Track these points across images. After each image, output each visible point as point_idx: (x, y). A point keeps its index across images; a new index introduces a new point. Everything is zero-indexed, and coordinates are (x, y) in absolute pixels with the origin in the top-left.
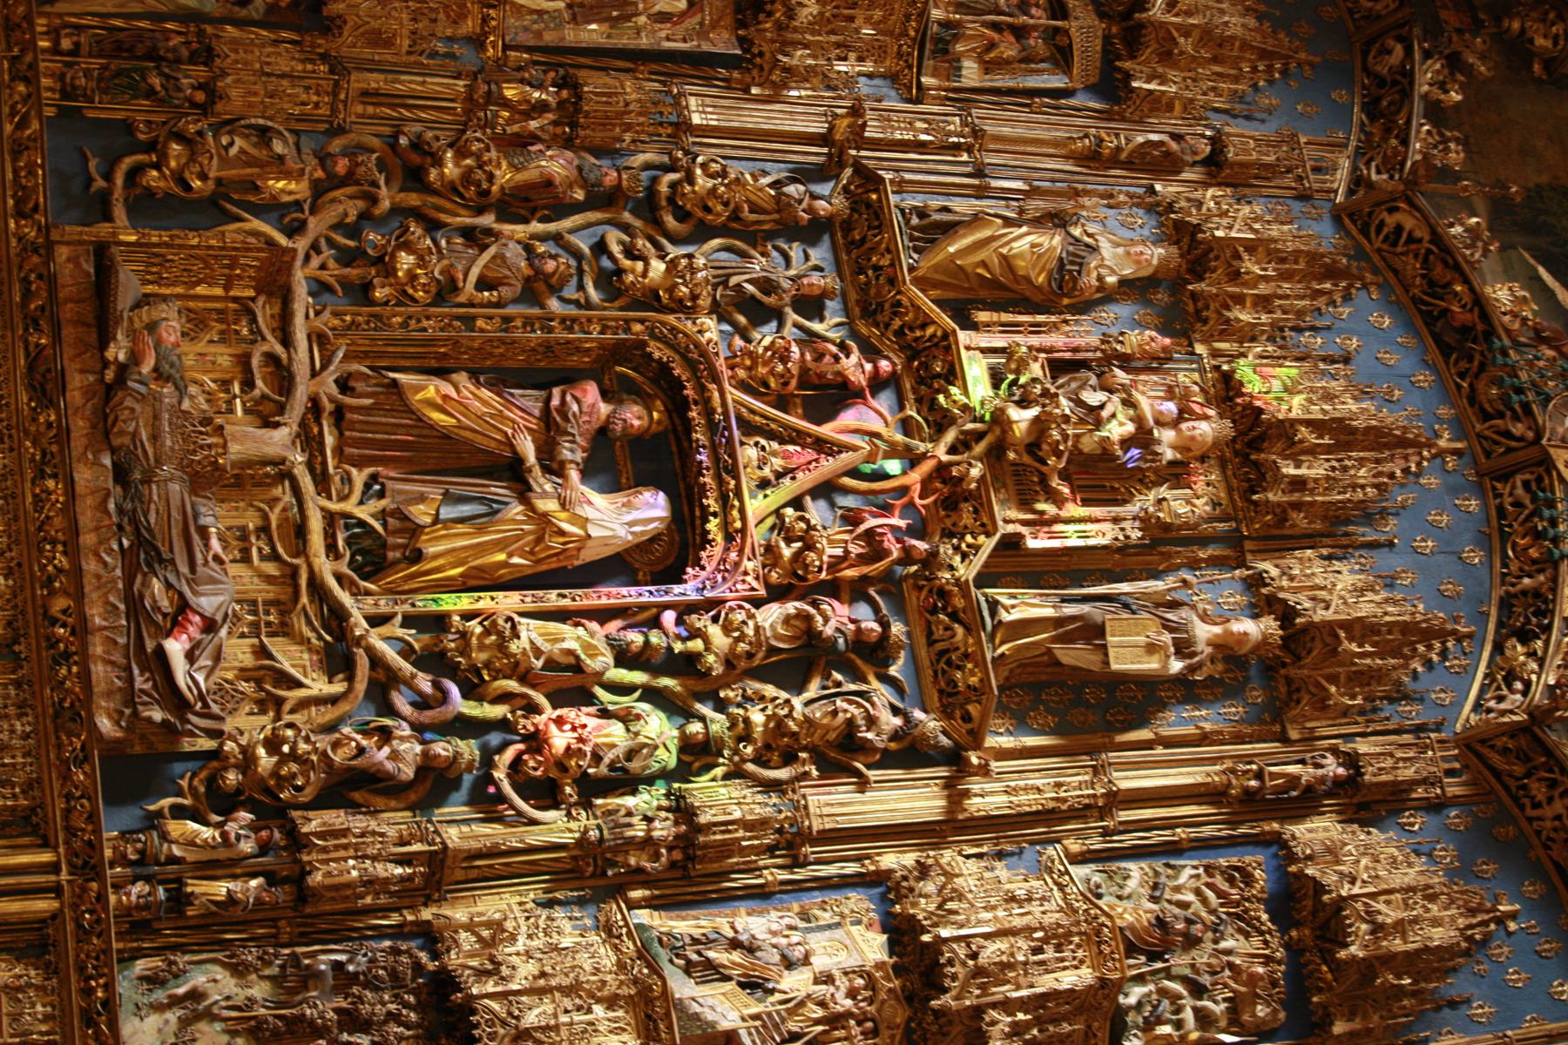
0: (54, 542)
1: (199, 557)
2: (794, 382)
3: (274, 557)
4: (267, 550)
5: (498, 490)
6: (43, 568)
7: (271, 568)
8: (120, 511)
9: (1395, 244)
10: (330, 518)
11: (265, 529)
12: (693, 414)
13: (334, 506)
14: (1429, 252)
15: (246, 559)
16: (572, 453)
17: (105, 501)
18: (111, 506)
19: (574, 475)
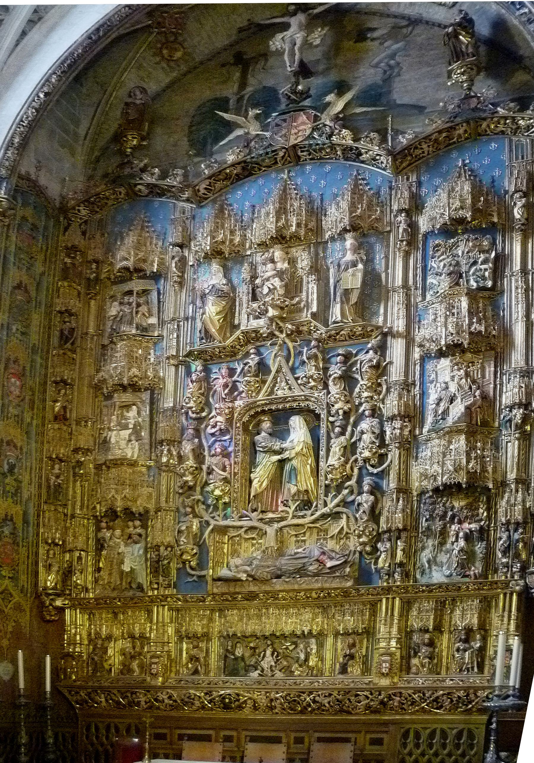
0: (297, 596)
1: (303, 555)
2: (257, 379)
3: (304, 533)
4: (302, 535)
5: (287, 467)
6: (304, 599)
7: (308, 534)
8: (288, 577)
9: (211, 190)
10: (294, 517)
11: (296, 536)
12: (266, 409)
13: (291, 516)
14: (214, 180)
15: (304, 541)
16: (277, 445)
17: (286, 582)
18: (287, 580)
19: (283, 446)
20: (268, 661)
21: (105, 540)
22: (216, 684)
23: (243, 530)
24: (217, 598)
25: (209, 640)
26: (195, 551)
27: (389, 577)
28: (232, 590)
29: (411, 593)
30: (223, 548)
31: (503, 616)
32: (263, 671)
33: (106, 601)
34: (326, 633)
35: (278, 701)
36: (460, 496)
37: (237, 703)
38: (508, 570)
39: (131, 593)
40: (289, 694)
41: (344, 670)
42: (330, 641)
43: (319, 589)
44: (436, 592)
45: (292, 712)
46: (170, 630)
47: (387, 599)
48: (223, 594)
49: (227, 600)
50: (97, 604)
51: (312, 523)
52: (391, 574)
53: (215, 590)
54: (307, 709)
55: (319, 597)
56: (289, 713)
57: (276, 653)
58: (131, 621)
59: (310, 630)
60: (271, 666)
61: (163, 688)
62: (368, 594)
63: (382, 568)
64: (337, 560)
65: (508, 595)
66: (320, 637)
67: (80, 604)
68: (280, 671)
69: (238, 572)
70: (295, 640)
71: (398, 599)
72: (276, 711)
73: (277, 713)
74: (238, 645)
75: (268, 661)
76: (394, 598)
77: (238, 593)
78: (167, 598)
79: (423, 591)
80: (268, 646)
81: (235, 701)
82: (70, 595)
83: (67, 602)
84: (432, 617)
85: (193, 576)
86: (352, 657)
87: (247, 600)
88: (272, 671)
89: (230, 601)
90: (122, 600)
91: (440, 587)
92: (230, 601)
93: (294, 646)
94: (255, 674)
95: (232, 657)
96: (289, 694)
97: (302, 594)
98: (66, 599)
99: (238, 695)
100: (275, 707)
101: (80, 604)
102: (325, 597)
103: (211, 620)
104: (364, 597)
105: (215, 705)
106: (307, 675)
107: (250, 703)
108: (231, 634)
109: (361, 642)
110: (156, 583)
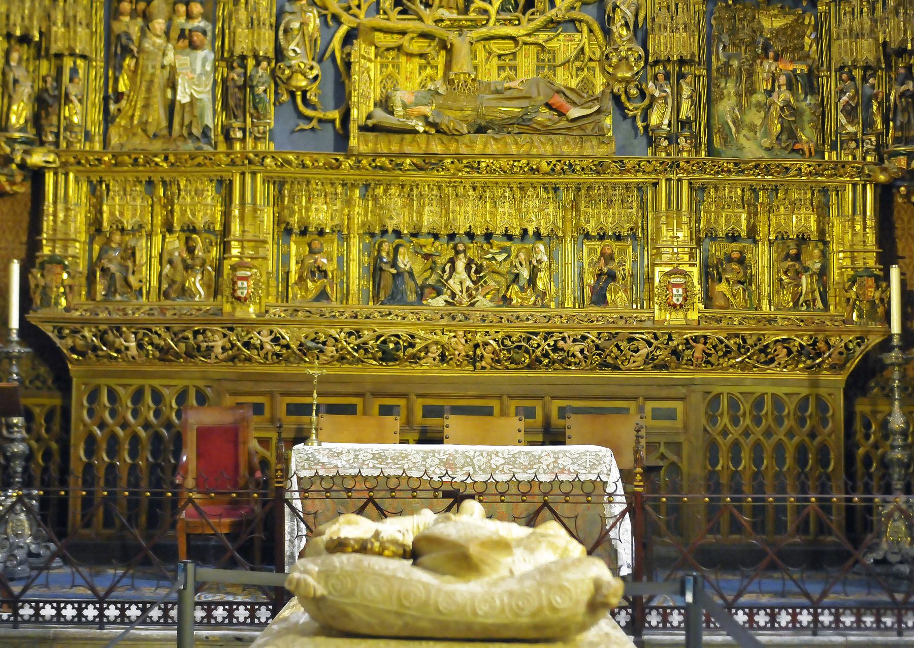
20: (460, 280)
21: (129, 38)
22: (367, 318)
23: (407, 37)
24: (364, 162)
25: (344, 237)
26: (315, 72)
27: (669, 144)
28: (395, 148)
29: (709, 173)
30: (368, 70)
31: (853, 221)
32: (453, 295)
33: (136, 160)
34: (561, 234)
35: (489, 347)
36: (772, 12)
37: (410, 351)
38: (858, 147)
39: (190, 146)
40: (510, 337)
41: (600, 298)
42: (569, 246)
43: (554, 155)
44: (748, 175)
45: (513, 366)
46: (267, 217)
47: (668, 180)
48: (376, 155)
49: (381, 168)
50: (116, 165)
51: (529, 35)
52: (672, 139)
53: (363, 149)
54: (541, 362)
55: (553, 170)
56: (507, 368)
57: (474, 266)
58: (188, 200)
59: (538, 229)
60: (468, 288)
61: (262, 321)
62: (638, 171)
63: (658, 127)
64: (581, 106)
65: (859, 188)
66: (552, 238)
67: (79, 163)
68: (484, 297)
69: (408, 116)
70: (508, 244)
71: (685, 183)
72: (483, 363)
73: (483, 368)
74: (401, 250)
75: (460, 280)
76: (679, 180)
77: (407, 155)
78: (263, 159)
79: (729, 171)
80: (457, 253)
81: (406, 348)
82: (57, 144)
83: (51, 158)
84: (744, 216)
85: (309, 119)
86: (612, 276)
87: (421, 169)
88: (470, 296)
89: (388, 170)
90: (172, 159)
91: (756, 166)
92: (388, 170)
93: (504, 255)
94: (439, 302)
95: (393, 271)
96: (510, 337)
97: (524, 161)
98: (50, 152)
99: (413, 337)
100: (482, 357)
101: (79, 163)
102: (564, 171)
103: (348, 202)
104: (630, 176)
105: (366, 351)
106: (535, 304)
107: (435, 351)
108: (390, 230)
109: (622, 251)
110: (240, 129)
